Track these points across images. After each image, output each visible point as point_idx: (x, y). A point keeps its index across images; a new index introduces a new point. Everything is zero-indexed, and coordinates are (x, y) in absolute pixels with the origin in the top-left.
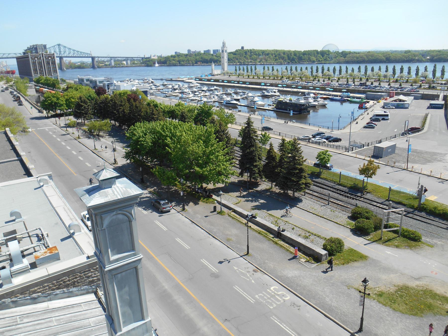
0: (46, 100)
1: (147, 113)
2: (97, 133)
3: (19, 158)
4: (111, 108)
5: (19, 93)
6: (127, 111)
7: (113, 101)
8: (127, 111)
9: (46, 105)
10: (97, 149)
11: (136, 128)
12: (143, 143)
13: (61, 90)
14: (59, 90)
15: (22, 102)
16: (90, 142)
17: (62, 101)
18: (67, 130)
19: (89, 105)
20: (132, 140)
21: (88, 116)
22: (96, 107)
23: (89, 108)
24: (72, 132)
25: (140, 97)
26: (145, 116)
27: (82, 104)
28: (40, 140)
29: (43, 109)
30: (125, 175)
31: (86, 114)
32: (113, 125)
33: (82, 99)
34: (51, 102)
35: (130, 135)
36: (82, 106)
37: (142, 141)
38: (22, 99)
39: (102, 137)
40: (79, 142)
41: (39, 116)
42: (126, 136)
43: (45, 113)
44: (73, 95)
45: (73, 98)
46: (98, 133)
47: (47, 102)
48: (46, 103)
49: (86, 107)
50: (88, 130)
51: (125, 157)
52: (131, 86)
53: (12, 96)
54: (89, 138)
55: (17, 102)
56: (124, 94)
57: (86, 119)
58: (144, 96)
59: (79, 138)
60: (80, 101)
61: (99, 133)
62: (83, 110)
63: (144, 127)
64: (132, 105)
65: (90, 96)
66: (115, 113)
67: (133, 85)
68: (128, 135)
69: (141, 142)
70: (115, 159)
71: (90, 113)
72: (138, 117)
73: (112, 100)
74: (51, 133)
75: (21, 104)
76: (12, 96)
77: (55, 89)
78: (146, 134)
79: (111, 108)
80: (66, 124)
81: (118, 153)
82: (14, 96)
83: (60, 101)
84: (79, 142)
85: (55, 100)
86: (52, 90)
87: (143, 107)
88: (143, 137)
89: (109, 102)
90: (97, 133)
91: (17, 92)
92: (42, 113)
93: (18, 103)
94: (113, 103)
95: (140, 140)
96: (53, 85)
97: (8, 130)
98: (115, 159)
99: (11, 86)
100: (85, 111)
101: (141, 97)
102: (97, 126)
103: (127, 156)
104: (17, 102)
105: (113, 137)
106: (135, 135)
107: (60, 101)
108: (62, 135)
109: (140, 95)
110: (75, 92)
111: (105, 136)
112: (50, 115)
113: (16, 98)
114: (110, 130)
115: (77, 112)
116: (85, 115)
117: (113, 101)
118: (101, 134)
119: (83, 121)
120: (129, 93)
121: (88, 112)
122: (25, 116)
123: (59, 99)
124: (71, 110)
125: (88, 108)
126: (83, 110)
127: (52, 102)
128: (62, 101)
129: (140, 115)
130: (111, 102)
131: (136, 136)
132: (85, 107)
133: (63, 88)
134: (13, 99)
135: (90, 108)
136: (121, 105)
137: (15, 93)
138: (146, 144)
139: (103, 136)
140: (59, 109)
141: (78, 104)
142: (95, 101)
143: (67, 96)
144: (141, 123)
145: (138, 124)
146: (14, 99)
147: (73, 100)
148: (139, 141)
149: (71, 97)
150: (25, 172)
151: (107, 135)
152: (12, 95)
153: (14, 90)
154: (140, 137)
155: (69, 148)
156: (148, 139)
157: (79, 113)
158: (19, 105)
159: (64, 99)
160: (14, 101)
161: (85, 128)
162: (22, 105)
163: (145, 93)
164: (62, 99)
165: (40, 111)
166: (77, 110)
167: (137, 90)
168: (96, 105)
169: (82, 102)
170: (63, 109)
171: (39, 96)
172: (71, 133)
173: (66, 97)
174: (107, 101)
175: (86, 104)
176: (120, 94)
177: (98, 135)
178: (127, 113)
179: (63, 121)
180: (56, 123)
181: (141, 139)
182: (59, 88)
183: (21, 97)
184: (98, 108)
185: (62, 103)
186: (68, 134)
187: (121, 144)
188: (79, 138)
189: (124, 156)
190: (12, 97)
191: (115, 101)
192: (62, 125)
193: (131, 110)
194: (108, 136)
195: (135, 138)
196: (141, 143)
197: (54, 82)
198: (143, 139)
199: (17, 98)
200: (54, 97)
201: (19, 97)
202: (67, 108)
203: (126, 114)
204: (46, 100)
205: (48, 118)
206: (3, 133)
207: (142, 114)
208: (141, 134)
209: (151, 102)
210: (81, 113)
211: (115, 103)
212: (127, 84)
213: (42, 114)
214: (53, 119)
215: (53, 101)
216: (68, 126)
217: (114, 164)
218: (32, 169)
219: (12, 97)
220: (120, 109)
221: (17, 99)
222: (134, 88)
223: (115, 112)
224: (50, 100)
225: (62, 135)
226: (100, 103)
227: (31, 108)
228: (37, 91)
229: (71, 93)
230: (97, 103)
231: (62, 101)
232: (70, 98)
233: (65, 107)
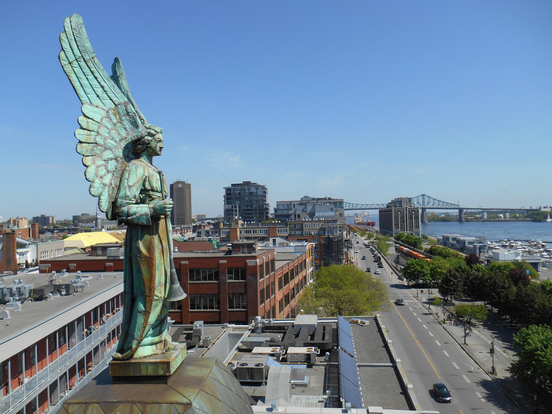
0: (409, 267)
1: (544, 306)
2: (467, 320)
3: (394, 364)
4: (488, 289)
5: (379, 253)
6: (511, 297)
7: (493, 280)
8: (511, 297)
9: (409, 273)
10: (467, 345)
11: (530, 332)
12: (542, 359)
13: (422, 251)
14: (421, 251)
15: (382, 264)
16: (458, 331)
17: (427, 270)
18: (429, 308)
19: (459, 281)
20: (524, 349)
21: (457, 294)
22: (467, 282)
23: (458, 285)
24: (436, 312)
25: (528, 272)
26: (541, 310)
27: (451, 279)
28: (399, 317)
29: (405, 278)
30: (508, 396)
31: (455, 291)
32: (489, 310)
33: (452, 272)
34: (415, 270)
35: (519, 340)
36: (451, 281)
37: (541, 355)
38: (382, 260)
39: (474, 326)
40: (444, 328)
41: (399, 284)
42: (515, 341)
43: (405, 282)
44: (440, 265)
45: (439, 268)
46: (469, 320)
47: (409, 270)
48: (409, 271)
49: (456, 283)
50: (457, 313)
51: (510, 370)
52: (514, 255)
53: (373, 255)
54: (457, 325)
55: (377, 263)
56: (505, 267)
57: (454, 297)
58: (534, 271)
59: (444, 323)
60: (449, 274)
61: (470, 320)
62: (451, 286)
63: (543, 335)
64: (521, 290)
65: (460, 267)
66: (493, 296)
67: (517, 254)
68: (517, 340)
69: (538, 357)
70: (493, 367)
71: (459, 290)
72: (530, 309)
73: (490, 279)
74: (411, 309)
75: (380, 266)
76: (373, 255)
77: (415, 249)
78: (546, 347)
79: (488, 289)
80: (429, 300)
81: (497, 357)
82: (375, 256)
83: (424, 270)
84: (444, 328)
85: (418, 268)
86: (413, 250)
87: (538, 296)
88: (542, 351)
89: (486, 281)
90: (467, 320)
91: (378, 251)
92: (403, 280)
93: (378, 264)
94: (492, 282)
95: (537, 354)
96: (415, 244)
97: (378, 316)
98: (493, 367)
99: (373, 243)
100: (453, 288)
101: (529, 272)
102: (469, 311)
103: (514, 369)
104: (377, 263)
105: (490, 329)
106: (529, 344)
107: (424, 270)
108: (423, 314)
109: (528, 269)
110: (443, 261)
111: (477, 324)
112: (411, 284)
113: (376, 259)
114: (485, 318)
115: (444, 287)
116: (453, 292)
117: (493, 280)
118: (473, 321)
119: (449, 299)
120: (513, 267)
121: (457, 289)
122: (385, 282)
123: (424, 268)
124: (435, 282)
125: (458, 284)
126: (451, 286)
127: (415, 271)
128: (427, 270)
129: (531, 307)
130: (489, 281)
131: (531, 346)
132: (454, 283)
133: (426, 249)
134: (373, 259)
135: (460, 284)
136: (503, 287)
137: (376, 252)
138: (546, 361)
139: (476, 325)
140: (422, 280)
141: (446, 278)
142: (466, 275)
143: (433, 264)
144: (538, 326)
145: (534, 327)
146: (374, 259)
147: (439, 270)
148: (535, 355)
149: (437, 266)
150: (402, 389)
151: (482, 323)
152: (373, 254)
153: (375, 248)
154: (537, 349)
155: (432, 335)
156: (549, 354)
157: (446, 289)
158: (378, 267)
159: (429, 268)
160: (374, 261)
161: (452, 309)
162: (382, 267)
163: (535, 265)
164: (427, 268)
165: (400, 278)
166: (444, 285)
167: (523, 262)
168: (467, 280)
169: (451, 276)
170: (426, 279)
171: (398, 256)
172: (434, 314)
173: (431, 265)
174: (483, 279)
175: (456, 280)
176: (499, 267)
177: (469, 323)
178: (512, 300)
179: (425, 295)
180: (417, 297)
181: (539, 352)
182: (421, 248)
183: (382, 258)
184: (469, 284)
185: (426, 272)
186: (431, 314)
187: (500, 342)
188: (444, 323)
189: (509, 369)
190: (373, 257)
191: (494, 281)
192: (425, 300)
193: (517, 297)
194: (482, 325)
195: (527, 348)
196: (538, 359)
197: (416, 240)
198: (541, 353)
199: (378, 258)
200: (418, 265)
201: (380, 258)
202: (431, 279)
203: (511, 301)
204: (409, 267)
205: (408, 287)
206: (373, 318)
207: (536, 306)
208: (539, 345)
209: (547, 285)
210: (448, 289)
211: (495, 283)
212: (509, 252)
213: (402, 282)
214: (414, 290)
215: (417, 269)
216: (431, 302)
217: (491, 373)
218: (410, 389)
219: (373, 257)
220: (501, 292)
221: (378, 260)
222: (519, 258)
223: (494, 294)
224: (413, 268)
225: (423, 314)
226: (474, 279)
227: (392, 273)
228: (397, 249)
229: (437, 262)
230: (468, 277)
231: (427, 270)
232: (436, 267)
233: (428, 277)
